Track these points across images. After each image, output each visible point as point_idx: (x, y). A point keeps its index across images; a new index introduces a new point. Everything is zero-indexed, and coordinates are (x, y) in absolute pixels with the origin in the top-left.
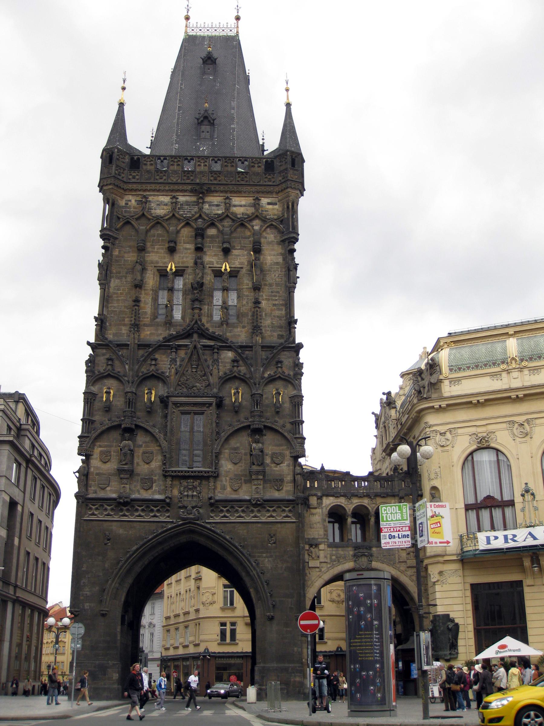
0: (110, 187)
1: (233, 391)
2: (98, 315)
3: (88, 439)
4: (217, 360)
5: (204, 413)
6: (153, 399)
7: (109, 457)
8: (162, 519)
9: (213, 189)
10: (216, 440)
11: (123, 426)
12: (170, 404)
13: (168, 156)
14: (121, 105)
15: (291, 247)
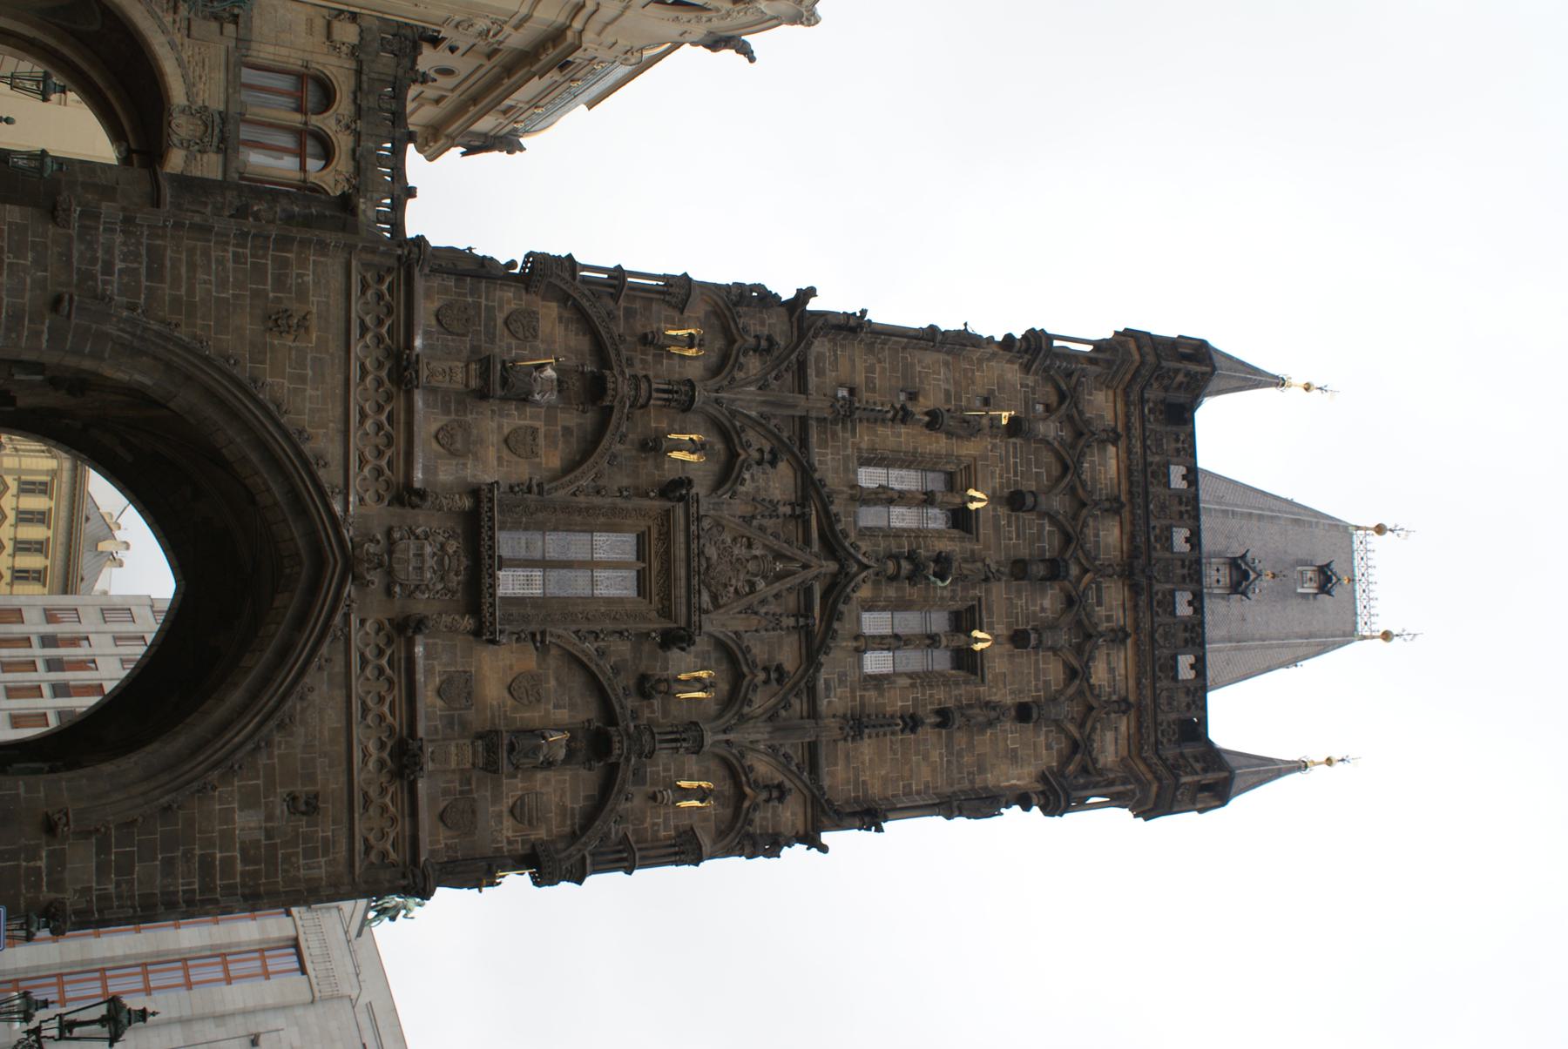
0: (1137, 357)
1: (703, 674)
2: (869, 321)
3: (569, 279)
4: (778, 626)
5: (644, 597)
6: (676, 455)
7: (520, 335)
8: (355, 484)
9: (1144, 598)
10: (577, 632)
11: (607, 372)
12: (668, 504)
13: (1197, 490)
14: (1278, 382)
15: (1035, 799)
